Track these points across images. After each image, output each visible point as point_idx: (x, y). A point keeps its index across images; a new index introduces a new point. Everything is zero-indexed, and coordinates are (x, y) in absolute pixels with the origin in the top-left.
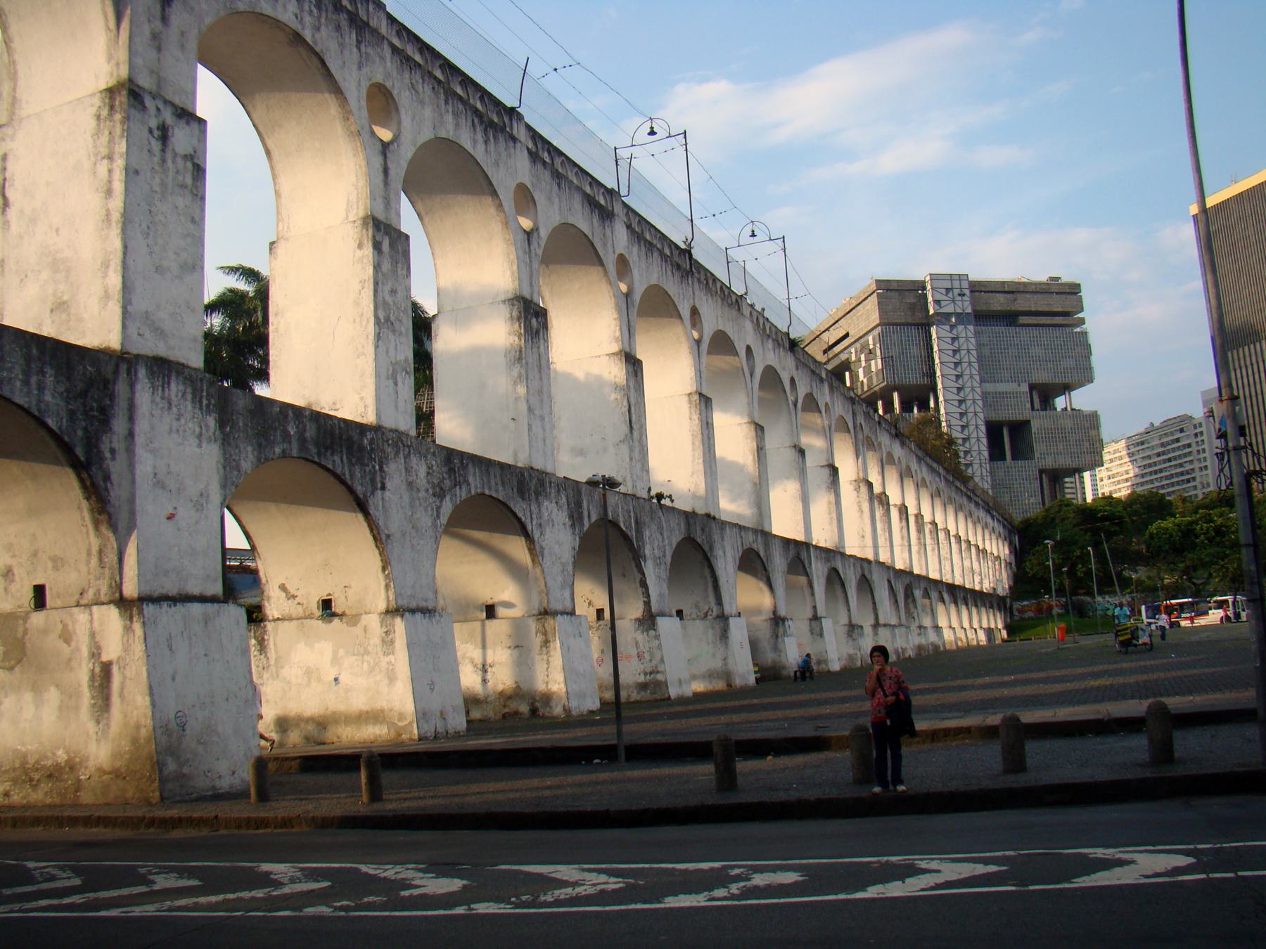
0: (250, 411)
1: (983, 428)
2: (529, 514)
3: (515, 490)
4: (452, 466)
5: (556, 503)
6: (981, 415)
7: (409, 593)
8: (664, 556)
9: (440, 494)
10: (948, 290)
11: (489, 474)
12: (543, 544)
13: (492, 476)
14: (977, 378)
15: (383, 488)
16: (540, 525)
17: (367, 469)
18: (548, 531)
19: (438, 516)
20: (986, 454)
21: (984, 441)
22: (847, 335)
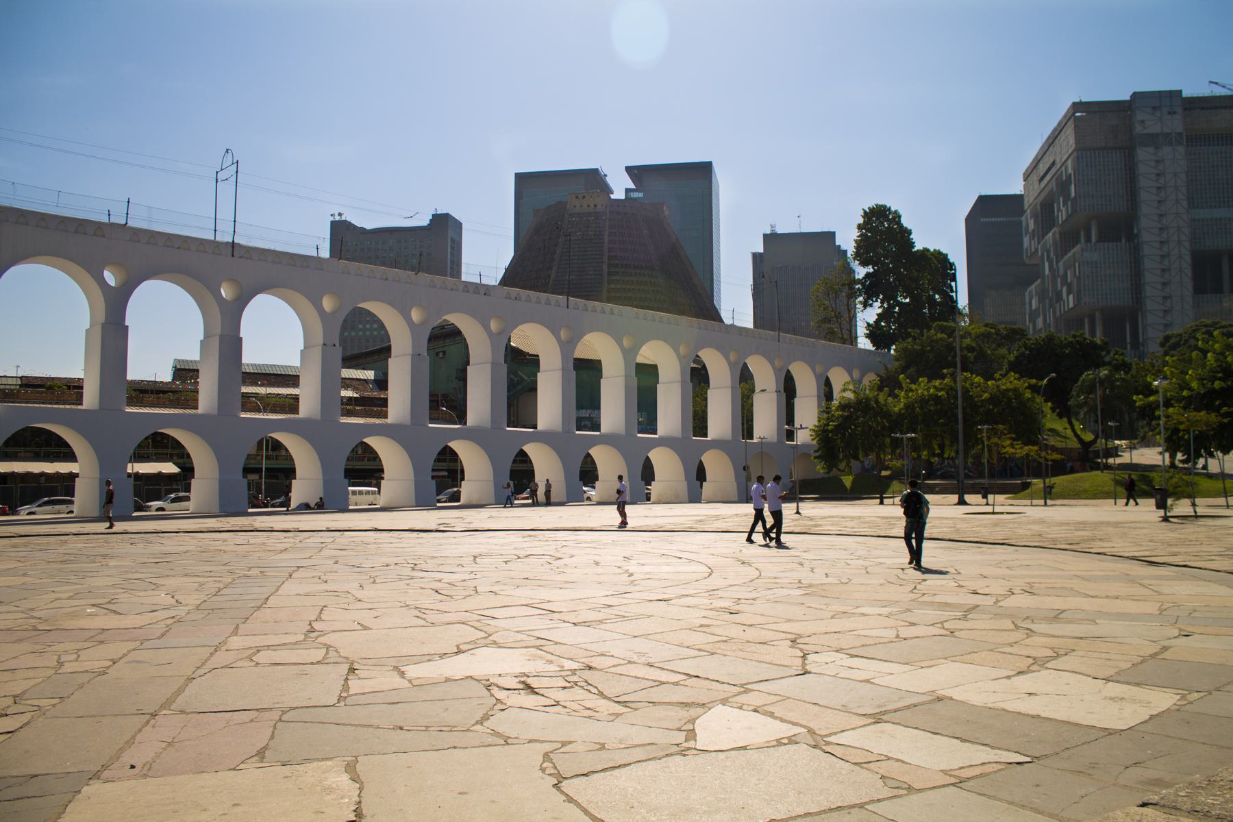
1: (1188, 258)
6: (1187, 244)
10: (1154, 108)
14: (1185, 203)
20: (1189, 285)
21: (1189, 272)
22: (1054, 163)
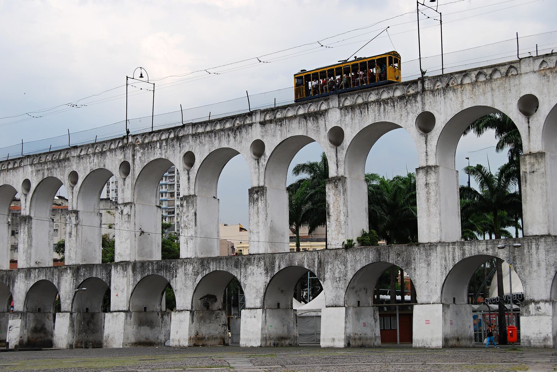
0: (140, 267)
2: (239, 273)
3: (233, 266)
4: (203, 264)
5: (257, 266)
7: (181, 306)
8: (346, 275)
9: (197, 274)
11: (220, 263)
12: (246, 283)
13: (222, 263)
15: (176, 277)
16: (245, 276)
17: (171, 273)
18: (250, 278)
19: (195, 281)
